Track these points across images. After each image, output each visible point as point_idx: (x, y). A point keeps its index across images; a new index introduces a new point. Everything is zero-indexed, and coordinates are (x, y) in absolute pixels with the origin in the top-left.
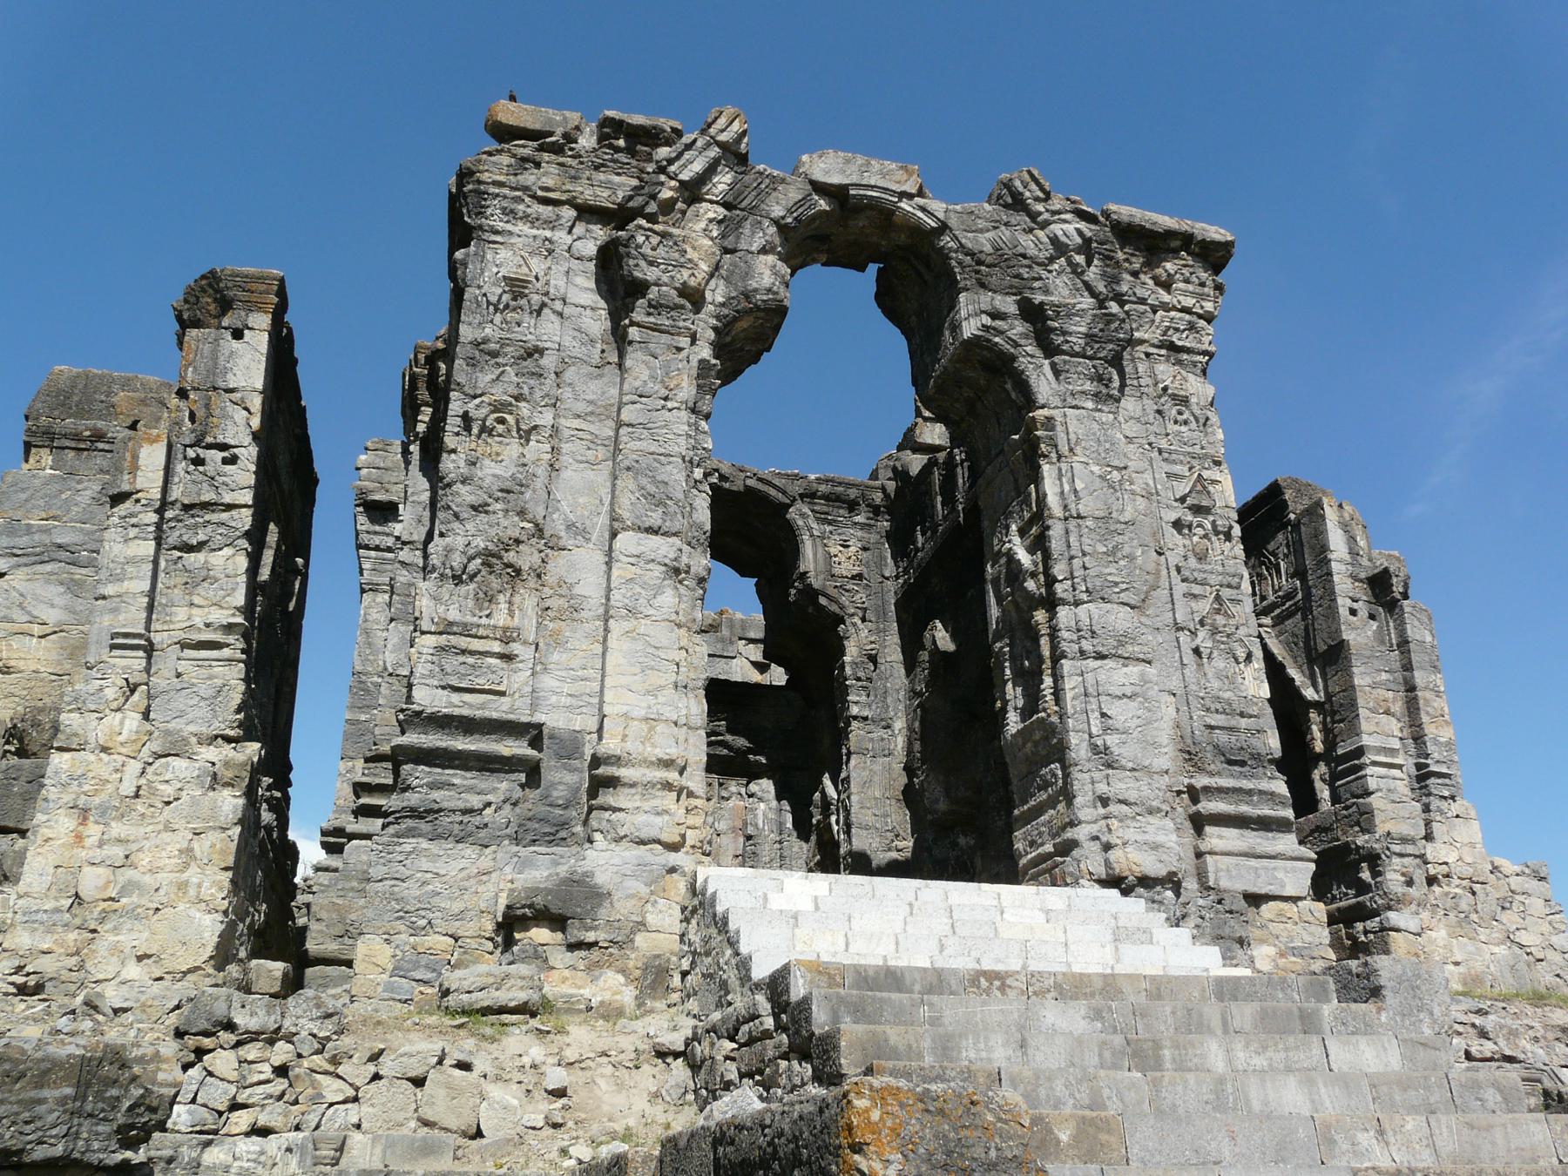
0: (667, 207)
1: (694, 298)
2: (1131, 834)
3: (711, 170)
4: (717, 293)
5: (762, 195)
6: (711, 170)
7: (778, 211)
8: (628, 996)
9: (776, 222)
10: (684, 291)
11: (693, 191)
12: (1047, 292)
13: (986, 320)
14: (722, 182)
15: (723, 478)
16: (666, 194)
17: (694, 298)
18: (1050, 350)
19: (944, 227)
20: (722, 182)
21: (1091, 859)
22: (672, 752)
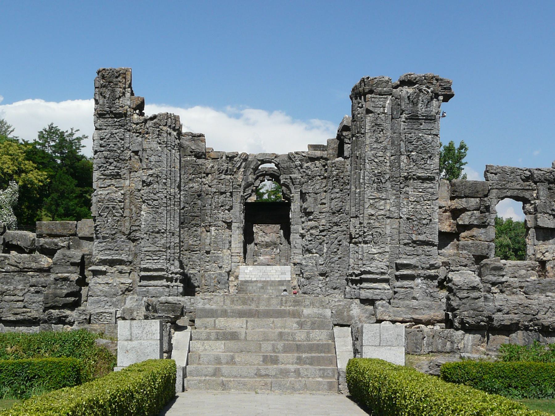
0: (235, 172)
1: (240, 186)
2: (297, 258)
3: (241, 163)
4: (243, 184)
5: (250, 165)
6: (241, 163)
7: (252, 167)
8: (234, 279)
9: (252, 169)
10: (238, 185)
11: (239, 168)
12: (294, 174)
13: (284, 180)
14: (244, 164)
15: (266, 172)
16: (235, 170)
17: (240, 186)
18: (294, 185)
19: (279, 164)
20: (244, 164)
21: (292, 261)
22: (238, 251)
